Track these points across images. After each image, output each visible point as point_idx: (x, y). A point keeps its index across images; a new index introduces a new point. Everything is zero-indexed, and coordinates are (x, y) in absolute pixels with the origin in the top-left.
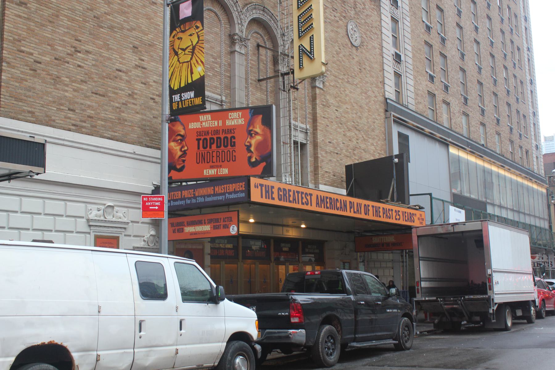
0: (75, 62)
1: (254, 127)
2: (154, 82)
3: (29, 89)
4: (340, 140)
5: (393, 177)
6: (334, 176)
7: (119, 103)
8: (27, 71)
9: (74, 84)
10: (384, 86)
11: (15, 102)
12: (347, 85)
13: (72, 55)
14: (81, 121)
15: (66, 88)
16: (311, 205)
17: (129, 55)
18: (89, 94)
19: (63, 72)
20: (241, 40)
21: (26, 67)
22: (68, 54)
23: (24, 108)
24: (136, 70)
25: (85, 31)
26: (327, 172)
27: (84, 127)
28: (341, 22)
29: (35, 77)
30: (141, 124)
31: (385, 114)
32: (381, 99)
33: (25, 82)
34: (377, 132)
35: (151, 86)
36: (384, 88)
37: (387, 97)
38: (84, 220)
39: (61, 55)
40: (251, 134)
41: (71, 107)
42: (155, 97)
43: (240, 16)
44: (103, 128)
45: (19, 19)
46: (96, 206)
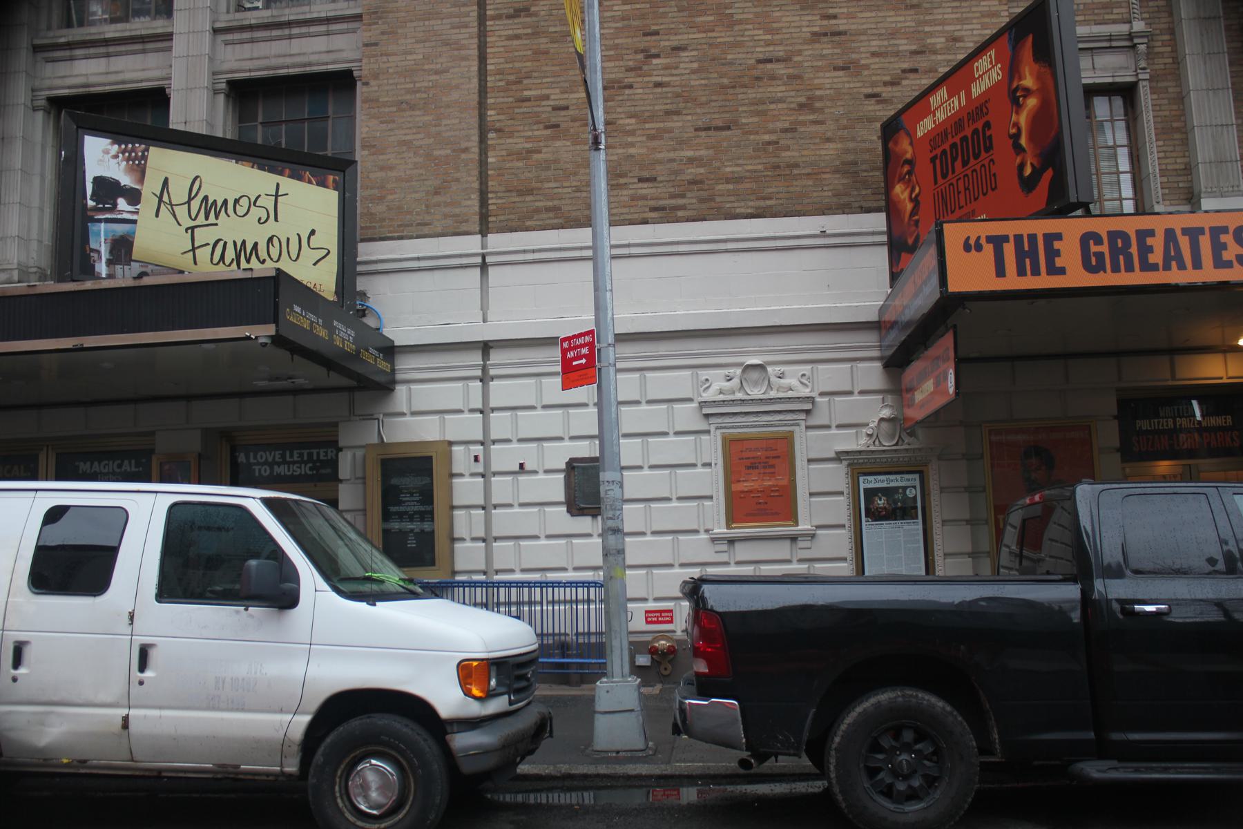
0: (646, 79)
1: (1020, 79)
2: (874, 54)
3: (546, 166)
7: (773, 132)
8: (537, 133)
9: (647, 126)
11: (517, 199)
13: (640, 69)
14: (672, 196)
15: (630, 139)
17: (789, 19)
18: (691, 133)
19: (619, 110)
21: (535, 127)
22: (629, 69)
23: (537, 204)
24: (817, 46)
25: (667, 10)
27: (683, 208)
29: (558, 138)
30: (843, 163)
33: (536, 156)
35: (867, 67)
38: (695, 405)
39: (613, 76)
40: (1016, 98)
41: (645, 174)
44: (732, 198)
45: (516, 42)
46: (725, 371)
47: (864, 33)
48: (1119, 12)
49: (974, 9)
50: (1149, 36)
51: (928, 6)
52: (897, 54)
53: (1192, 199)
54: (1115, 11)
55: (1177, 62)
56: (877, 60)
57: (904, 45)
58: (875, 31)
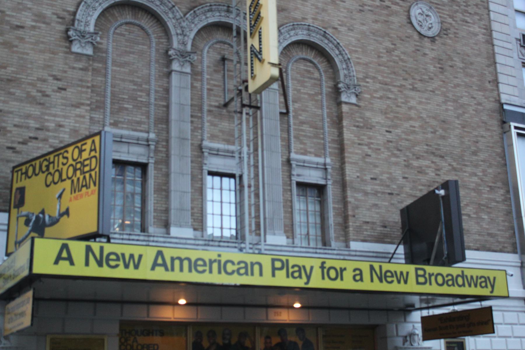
2: (15, 126)
4: (398, 172)
5: (440, 219)
6: (385, 227)
10: (497, 87)
12: (412, 94)
16: (261, 274)
20: (183, 55)
26: (368, 222)
28: (394, 8)
31: (502, 128)
32: (491, 105)
34: (482, 156)
35: (10, 132)
36: (498, 90)
37: (503, 101)
42: (14, 145)
43: (180, 23)
47: (11, 113)
48: (144, 127)
49: (72, 112)
50: (157, 142)
51: (49, 105)
52: (28, 128)
53: (167, 225)
54: (143, 126)
55: (168, 156)
56: (16, 129)
57: (33, 124)
58: (17, 113)
